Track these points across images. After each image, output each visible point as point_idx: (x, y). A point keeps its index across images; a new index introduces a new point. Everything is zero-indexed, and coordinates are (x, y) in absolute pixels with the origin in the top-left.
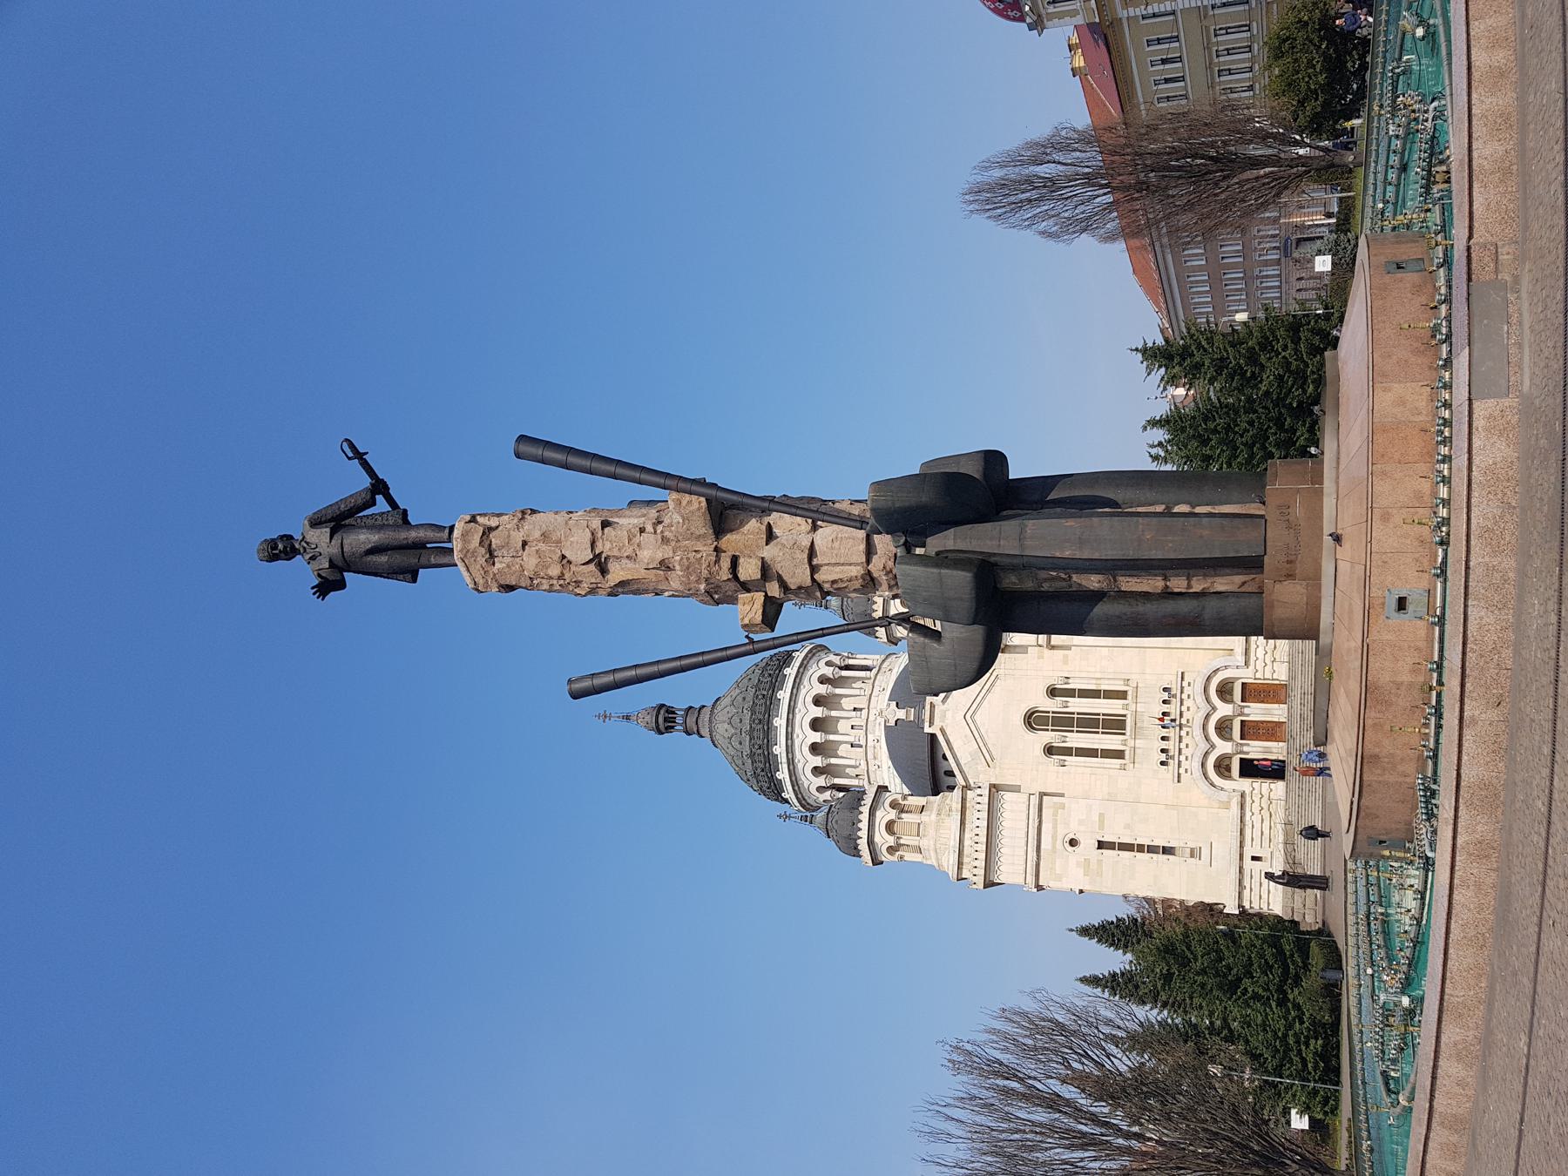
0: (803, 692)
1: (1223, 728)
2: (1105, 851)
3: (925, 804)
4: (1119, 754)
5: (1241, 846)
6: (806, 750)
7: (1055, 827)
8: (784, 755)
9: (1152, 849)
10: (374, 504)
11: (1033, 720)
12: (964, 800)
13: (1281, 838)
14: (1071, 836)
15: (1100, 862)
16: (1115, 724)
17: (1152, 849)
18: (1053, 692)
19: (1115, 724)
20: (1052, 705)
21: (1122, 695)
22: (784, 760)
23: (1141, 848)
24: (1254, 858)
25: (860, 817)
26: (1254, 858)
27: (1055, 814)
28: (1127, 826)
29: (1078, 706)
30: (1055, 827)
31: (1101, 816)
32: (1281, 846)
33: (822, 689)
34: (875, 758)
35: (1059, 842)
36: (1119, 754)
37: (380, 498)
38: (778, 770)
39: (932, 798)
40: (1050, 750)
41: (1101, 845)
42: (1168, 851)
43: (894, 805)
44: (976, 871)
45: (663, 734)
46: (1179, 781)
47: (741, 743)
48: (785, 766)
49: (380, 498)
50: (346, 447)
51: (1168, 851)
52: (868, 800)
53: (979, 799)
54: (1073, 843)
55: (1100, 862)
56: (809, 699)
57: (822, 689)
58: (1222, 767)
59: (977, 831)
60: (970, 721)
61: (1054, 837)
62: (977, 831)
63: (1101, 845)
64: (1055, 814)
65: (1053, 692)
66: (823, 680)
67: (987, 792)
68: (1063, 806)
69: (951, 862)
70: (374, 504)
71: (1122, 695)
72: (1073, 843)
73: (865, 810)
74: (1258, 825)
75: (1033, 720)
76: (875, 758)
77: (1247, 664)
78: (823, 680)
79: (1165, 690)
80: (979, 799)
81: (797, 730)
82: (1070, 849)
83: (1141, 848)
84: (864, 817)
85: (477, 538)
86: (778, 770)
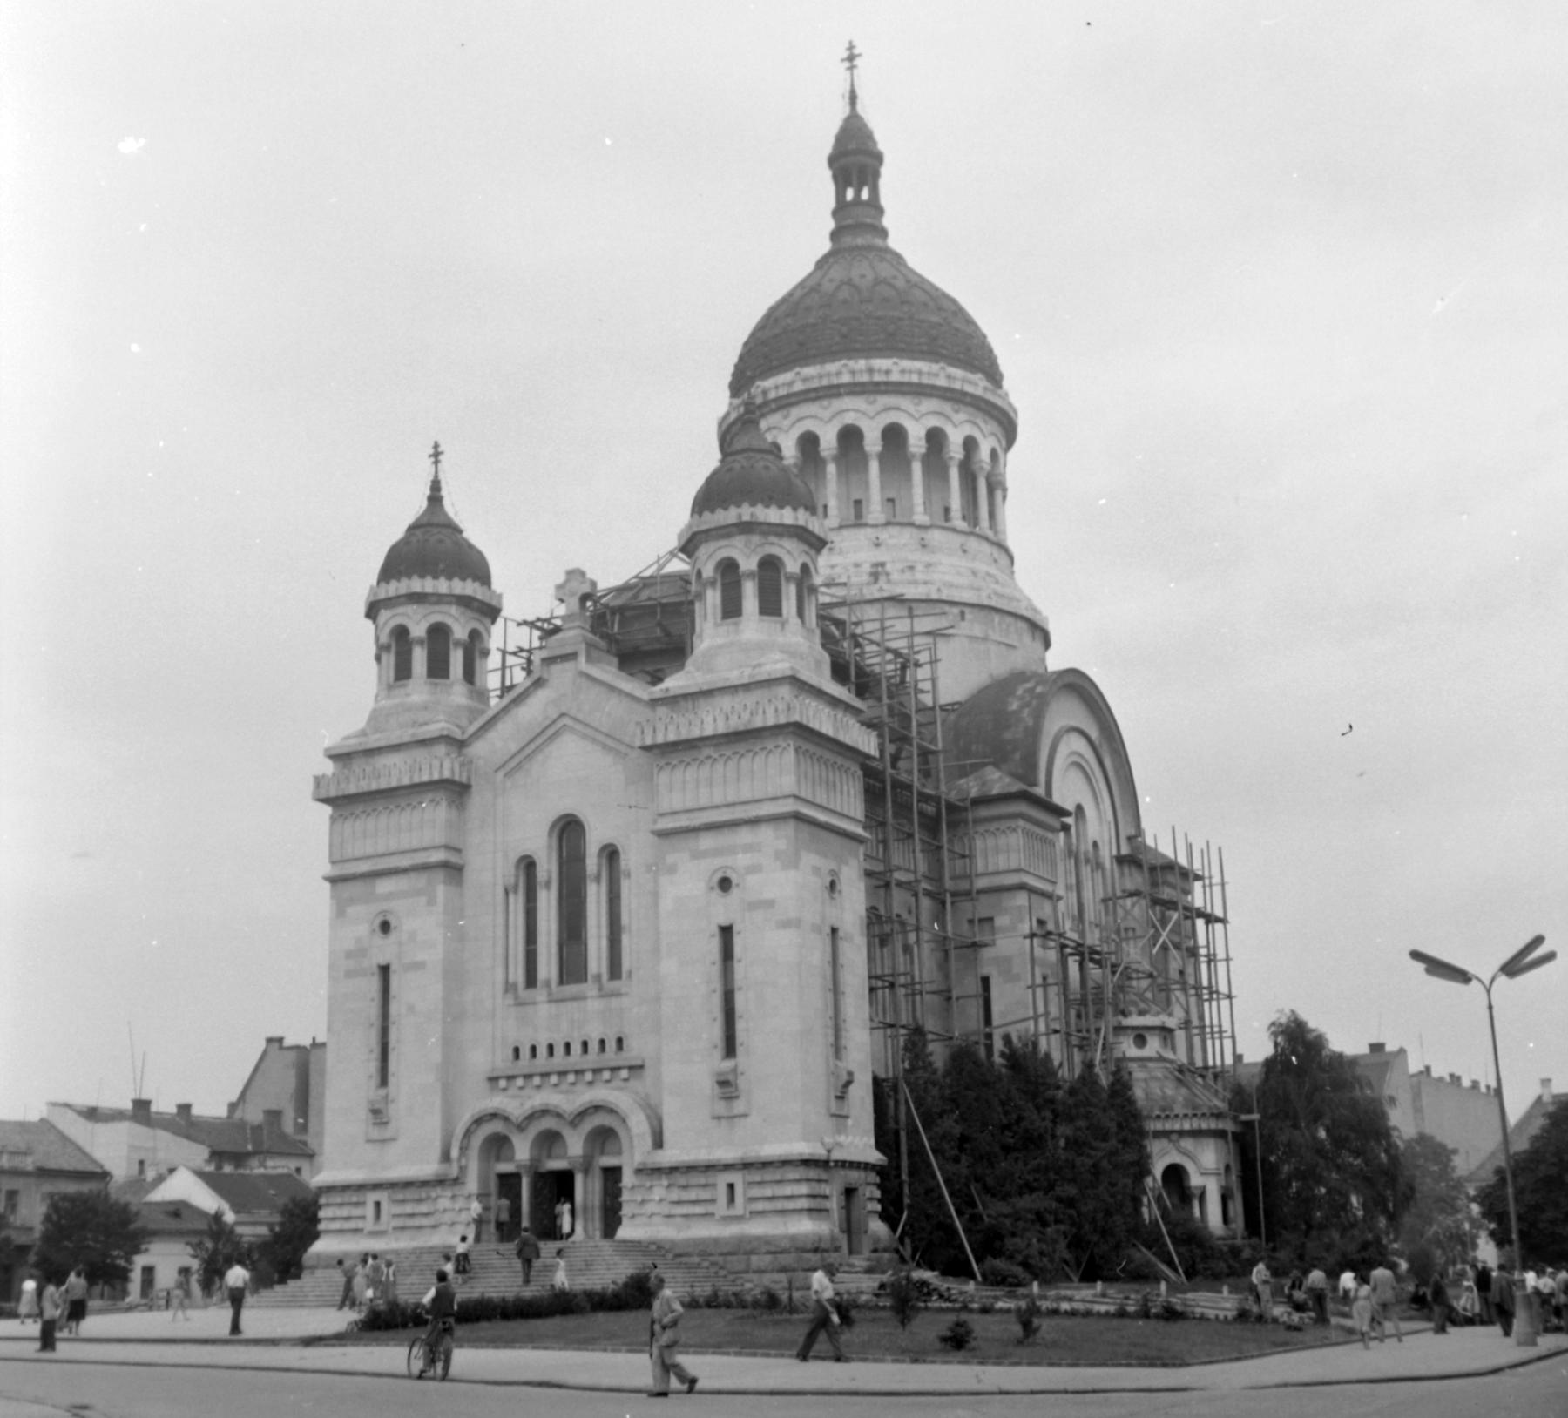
0: (905, 402)
4: (531, 980)
11: (569, 829)
14: (393, 923)
16: (572, 968)
19: (572, 968)
20: (592, 862)
21: (615, 970)
33: (916, 441)
36: (531, 980)
40: (528, 865)
41: (385, 970)
54: (385, 927)
56: (849, 419)
57: (916, 441)
58: (498, 1145)
60: (559, 725)
65: (611, 854)
66: (935, 438)
72: (385, 927)
75: (569, 829)
79: (620, 1041)
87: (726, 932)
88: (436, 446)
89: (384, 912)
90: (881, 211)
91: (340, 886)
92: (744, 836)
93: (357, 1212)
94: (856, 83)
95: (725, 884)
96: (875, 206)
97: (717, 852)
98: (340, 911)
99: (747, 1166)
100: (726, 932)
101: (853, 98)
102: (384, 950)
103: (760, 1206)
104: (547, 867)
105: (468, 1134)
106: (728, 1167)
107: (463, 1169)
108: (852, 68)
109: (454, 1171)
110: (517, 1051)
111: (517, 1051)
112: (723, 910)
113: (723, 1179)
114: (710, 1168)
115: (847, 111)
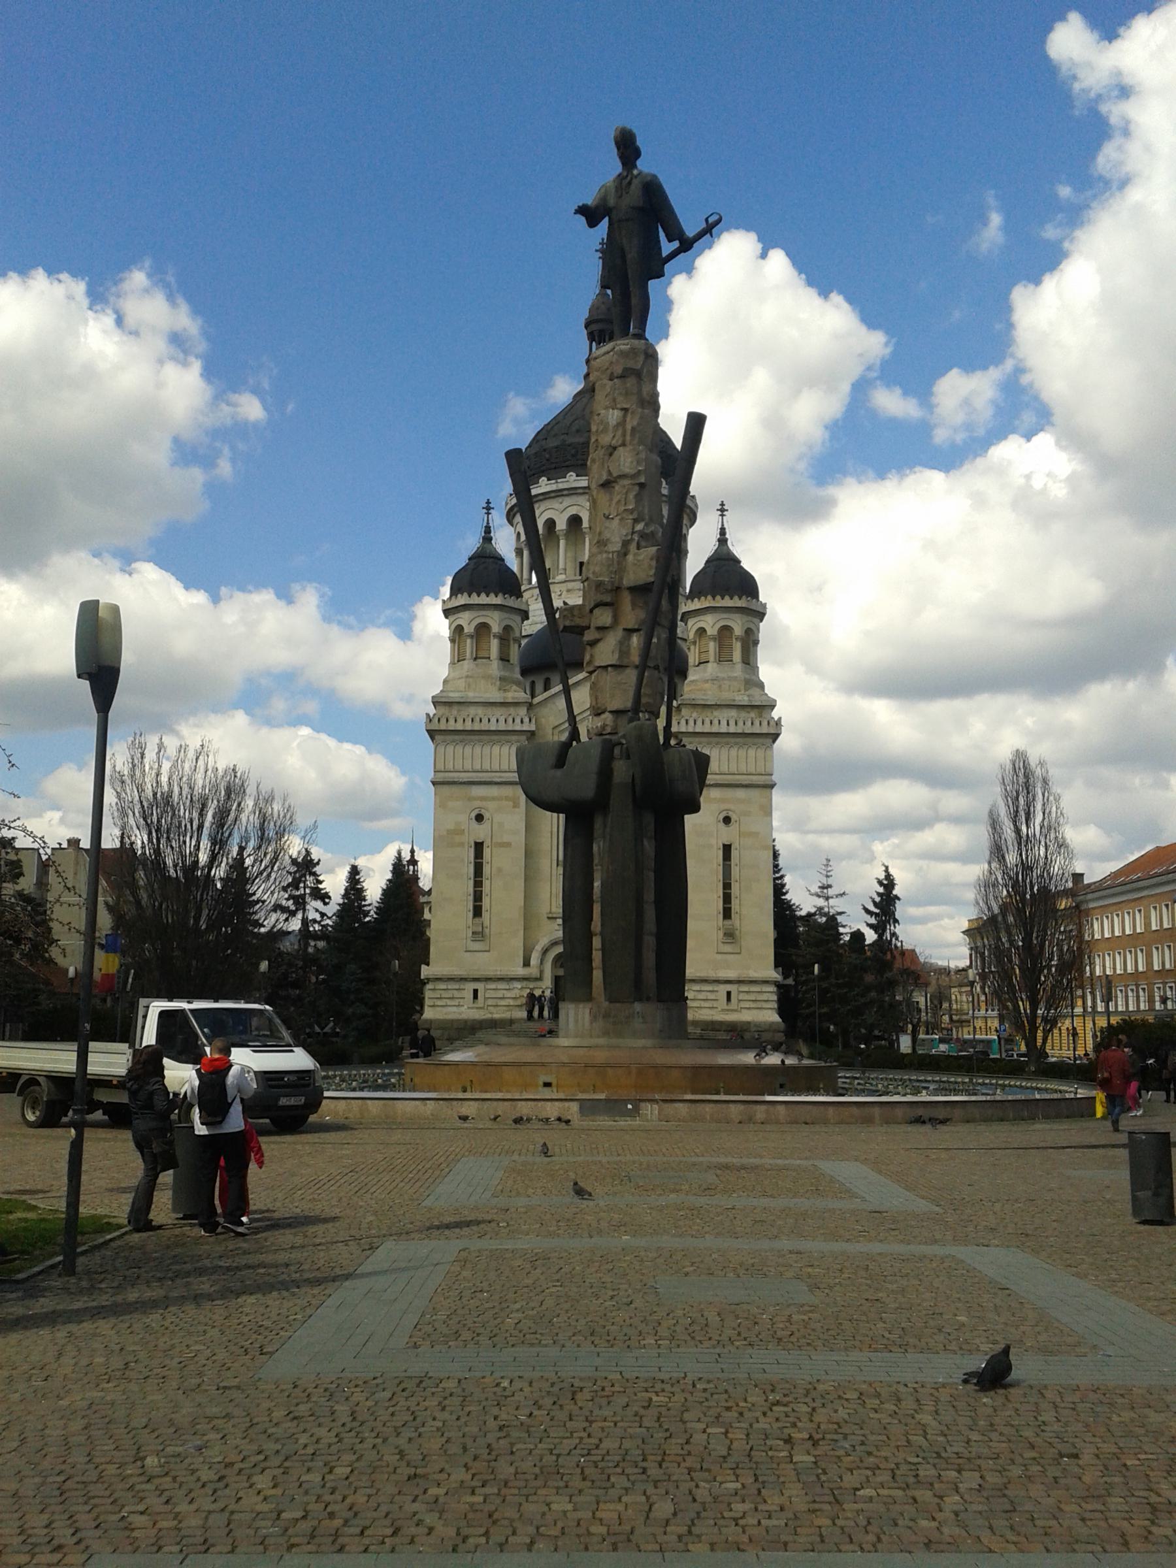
2: (472, 851)
3: (511, 662)
5: (488, 979)
6: (573, 511)
7: (493, 799)
8: (565, 486)
9: (478, 897)
10: (670, 241)
12: (516, 704)
13: (496, 1016)
15: (462, 844)
17: (478, 897)
22: (561, 486)
23: (478, 884)
25: (492, 595)
26: (476, 992)
27: (507, 798)
28: (500, 870)
30: (493, 799)
31: (508, 845)
32: (489, 1016)
34: (568, 591)
35: (477, 803)
37: (676, 244)
38: (549, 480)
39: (517, 670)
41: (479, 847)
42: (478, 912)
43: (507, 629)
44: (443, 721)
45: (586, 327)
46: (548, 918)
47: (578, 431)
48: (554, 487)
49: (676, 244)
50: (715, 218)
51: (478, 912)
52: (511, 602)
53: (518, 721)
55: (462, 844)
59: (485, 720)
61: (483, 799)
62: (485, 720)
63: (479, 847)
64: (507, 798)
67: (526, 727)
68: (516, 805)
69: (451, 695)
70: (670, 240)
72: (479, 818)
73: (498, 600)
74: (508, 994)
76: (568, 591)
80: (518, 721)
82: (473, 815)
83: (478, 884)
84: (493, 599)
85: (630, 364)
86: (549, 480)
87: (727, 849)
88: (488, 502)
92: (741, 793)
95: (727, 820)
97: (723, 801)
99: (740, 982)
100: (727, 849)
102: (480, 832)
103: (747, 1005)
105: (545, 952)
107: (541, 972)
109: (533, 971)
112: (726, 834)
113: (722, 989)
114: (718, 981)
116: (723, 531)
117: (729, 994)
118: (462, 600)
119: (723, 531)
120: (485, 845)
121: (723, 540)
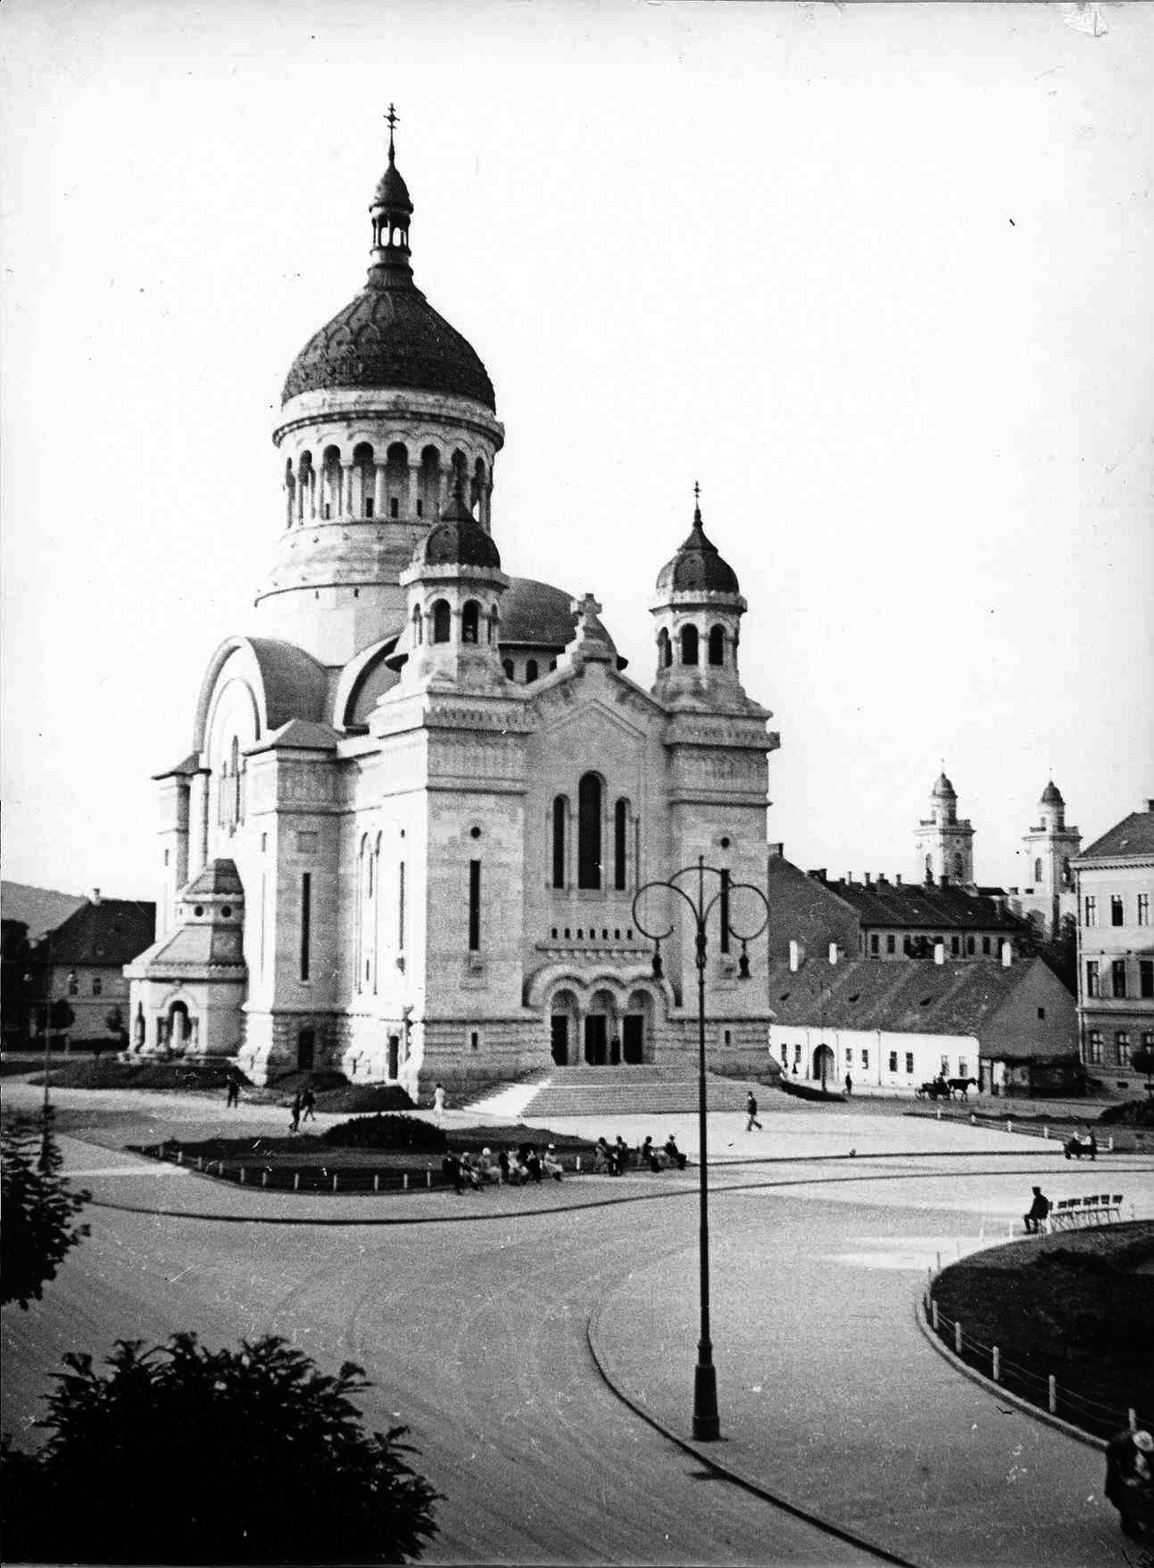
1: (604, 997)
11: (591, 785)
14: (482, 829)
16: (590, 878)
18: (621, 805)
19: (590, 878)
20: (608, 808)
21: (620, 885)
24: (475, 1037)
29: (608, 830)
33: (446, 459)
36: (558, 882)
40: (560, 802)
41: (475, 866)
56: (461, 445)
57: (446, 459)
58: (565, 997)
63: (475, 866)
65: (621, 805)
71: (620, 885)
75: (591, 785)
77: (671, 1021)
78: (459, 457)
81: (424, 428)
89: (473, 821)
90: (409, 253)
91: (434, 794)
93: (459, 1040)
94: (394, 144)
95: (725, 843)
96: (405, 250)
98: (435, 813)
101: (392, 154)
102: (477, 851)
104: (574, 807)
106: (728, 1021)
108: (392, 127)
110: (554, 932)
111: (554, 932)
115: (387, 164)
116: (698, 514)
117: (728, 1033)
118: (451, 570)
119: (698, 514)
120: (482, 866)
121: (698, 524)
